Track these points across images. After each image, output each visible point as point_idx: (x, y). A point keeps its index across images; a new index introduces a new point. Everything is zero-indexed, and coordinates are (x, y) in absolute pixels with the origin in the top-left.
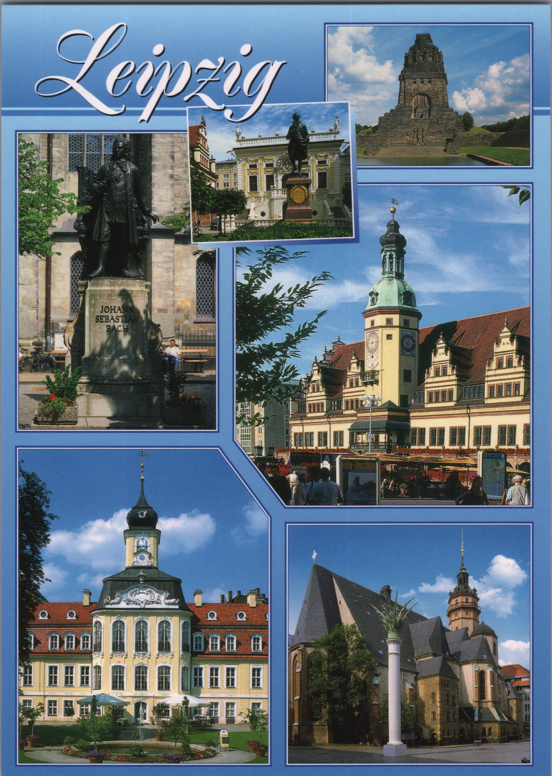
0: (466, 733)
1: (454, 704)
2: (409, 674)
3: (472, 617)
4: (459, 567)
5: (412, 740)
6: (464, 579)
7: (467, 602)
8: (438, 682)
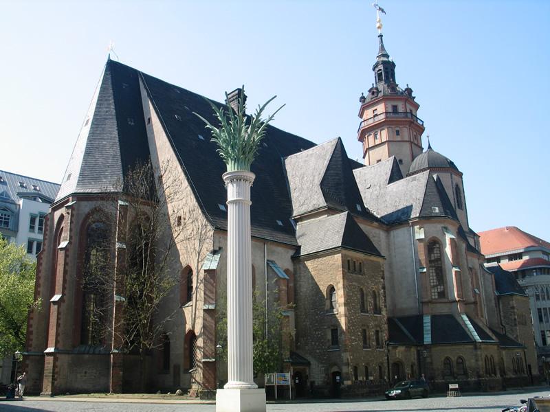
0: (408, 371)
1: (377, 310)
2: (280, 249)
3: (406, 138)
4: (377, 52)
5: (288, 386)
6: (386, 73)
8: (340, 263)
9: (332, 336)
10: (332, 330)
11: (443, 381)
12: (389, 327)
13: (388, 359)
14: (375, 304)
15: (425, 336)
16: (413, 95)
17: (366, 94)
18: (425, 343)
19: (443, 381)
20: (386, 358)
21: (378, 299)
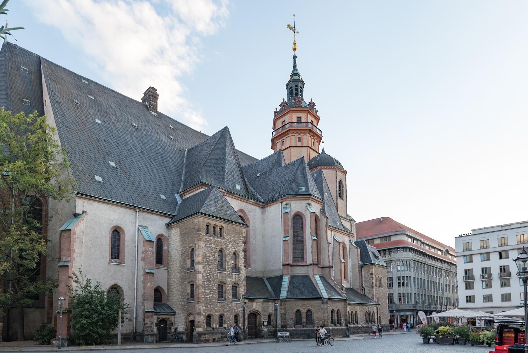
1: (236, 269)
7: (299, 122)
9: (191, 290)
10: (191, 285)
11: (294, 328)
12: (247, 283)
13: (244, 310)
14: (235, 264)
15: (282, 292)
16: (317, 107)
17: (279, 108)
18: (281, 298)
19: (294, 328)
20: (242, 309)
21: (237, 260)
